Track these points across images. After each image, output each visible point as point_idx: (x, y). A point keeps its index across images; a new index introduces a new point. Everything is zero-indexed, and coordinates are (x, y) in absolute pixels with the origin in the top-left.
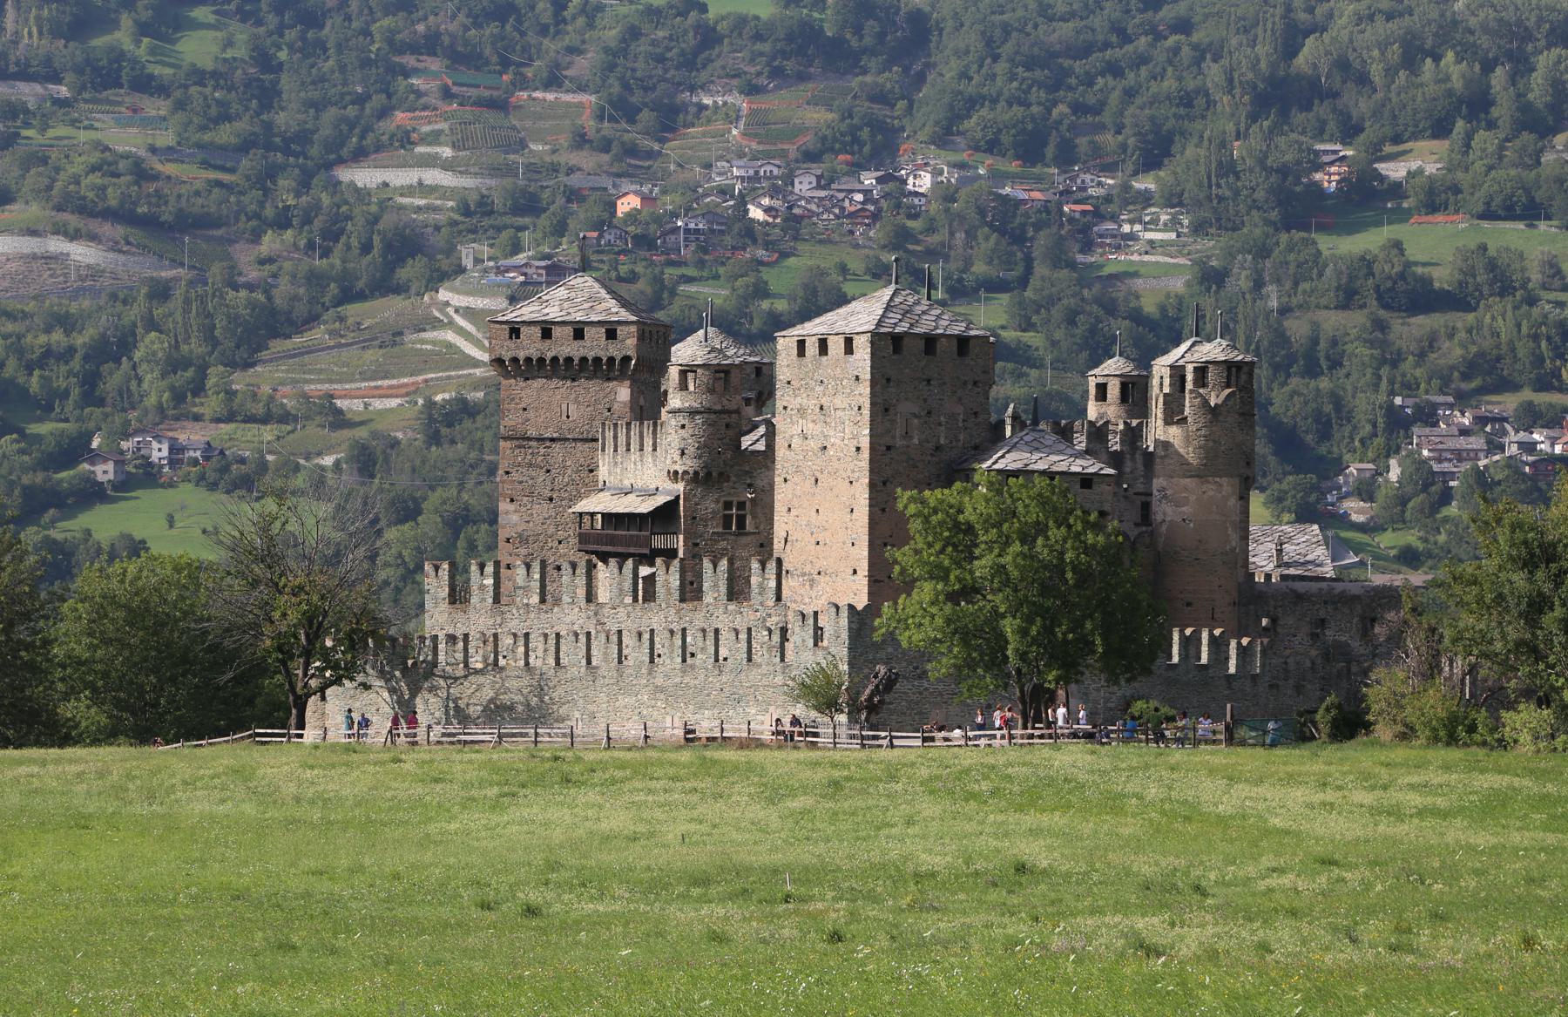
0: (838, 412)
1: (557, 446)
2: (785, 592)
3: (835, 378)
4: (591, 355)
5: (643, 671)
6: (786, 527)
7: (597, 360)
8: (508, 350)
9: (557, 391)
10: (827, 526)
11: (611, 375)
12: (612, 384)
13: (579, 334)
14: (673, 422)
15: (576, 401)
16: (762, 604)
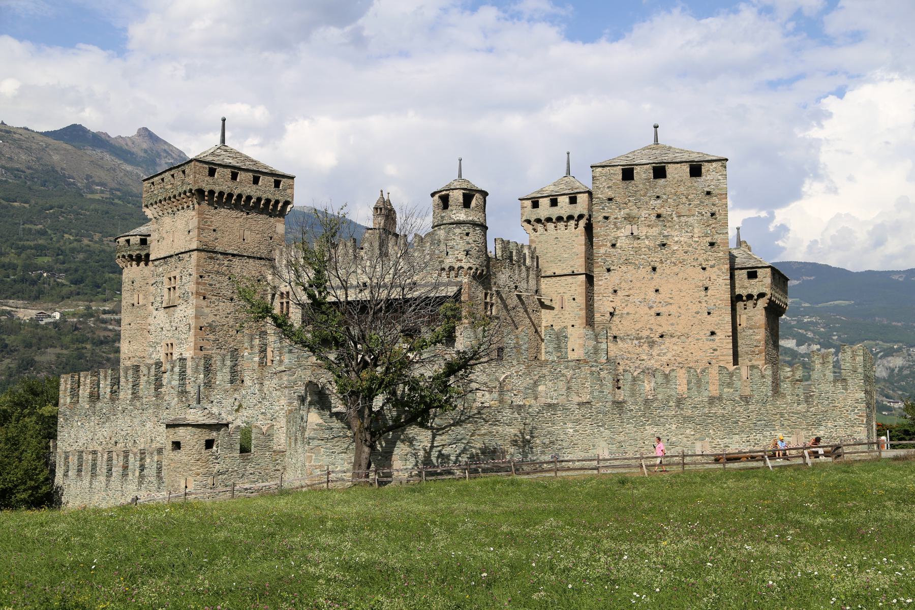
0: (683, 219)
1: (236, 261)
2: (611, 354)
3: (675, 194)
4: (264, 196)
5: (671, 403)
6: (613, 305)
7: (268, 201)
8: (206, 184)
9: (237, 220)
10: (671, 301)
12: (272, 220)
13: (256, 181)
14: (457, 231)
15: (249, 229)
16: (596, 361)
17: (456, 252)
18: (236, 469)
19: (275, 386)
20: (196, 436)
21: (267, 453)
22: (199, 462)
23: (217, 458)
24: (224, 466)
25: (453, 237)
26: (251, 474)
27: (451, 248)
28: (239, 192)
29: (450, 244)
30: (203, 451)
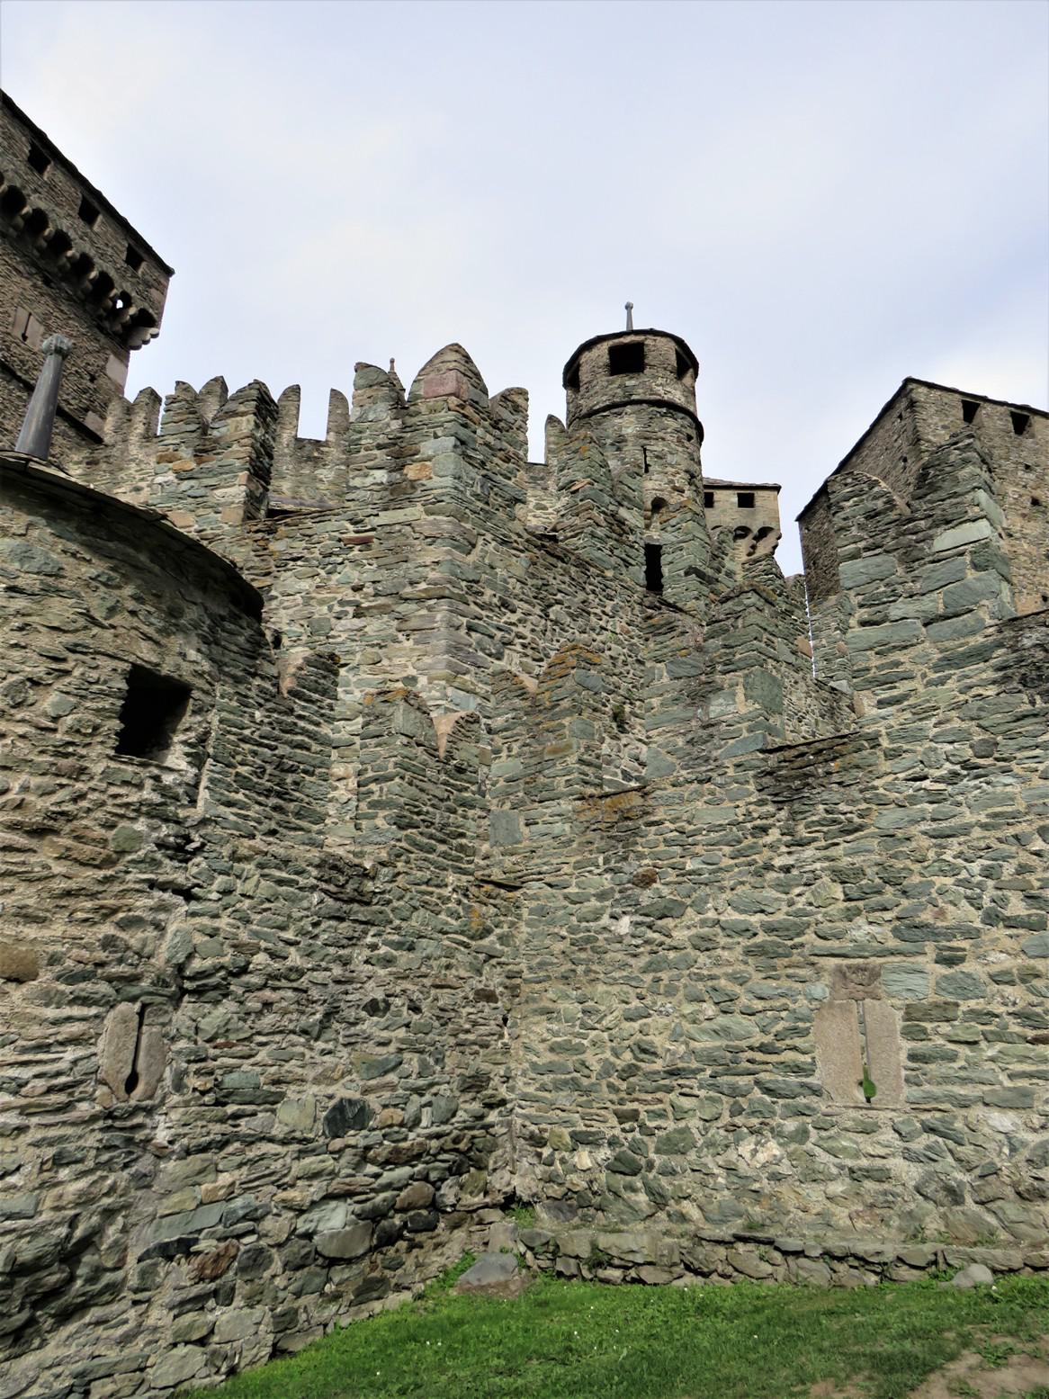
4: (101, 265)
9: (17, 279)
11: (107, 324)
17: (670, 469)
18: (295, 958)
19: (358, 597)
20: (59, 610)
21: (451, 878)
22: (45, 855)
23: (180, 851)
24: (224, 922)
25: (660, 434)
26: (373, 1008)
27: (657, 457)
28: (42, 205)
29: (655, 448)
30: (98, 758)
